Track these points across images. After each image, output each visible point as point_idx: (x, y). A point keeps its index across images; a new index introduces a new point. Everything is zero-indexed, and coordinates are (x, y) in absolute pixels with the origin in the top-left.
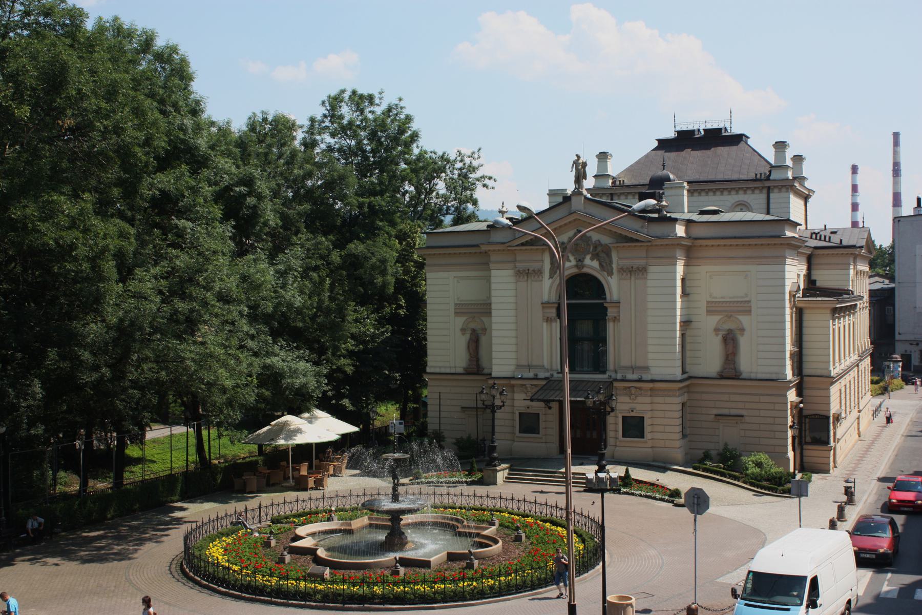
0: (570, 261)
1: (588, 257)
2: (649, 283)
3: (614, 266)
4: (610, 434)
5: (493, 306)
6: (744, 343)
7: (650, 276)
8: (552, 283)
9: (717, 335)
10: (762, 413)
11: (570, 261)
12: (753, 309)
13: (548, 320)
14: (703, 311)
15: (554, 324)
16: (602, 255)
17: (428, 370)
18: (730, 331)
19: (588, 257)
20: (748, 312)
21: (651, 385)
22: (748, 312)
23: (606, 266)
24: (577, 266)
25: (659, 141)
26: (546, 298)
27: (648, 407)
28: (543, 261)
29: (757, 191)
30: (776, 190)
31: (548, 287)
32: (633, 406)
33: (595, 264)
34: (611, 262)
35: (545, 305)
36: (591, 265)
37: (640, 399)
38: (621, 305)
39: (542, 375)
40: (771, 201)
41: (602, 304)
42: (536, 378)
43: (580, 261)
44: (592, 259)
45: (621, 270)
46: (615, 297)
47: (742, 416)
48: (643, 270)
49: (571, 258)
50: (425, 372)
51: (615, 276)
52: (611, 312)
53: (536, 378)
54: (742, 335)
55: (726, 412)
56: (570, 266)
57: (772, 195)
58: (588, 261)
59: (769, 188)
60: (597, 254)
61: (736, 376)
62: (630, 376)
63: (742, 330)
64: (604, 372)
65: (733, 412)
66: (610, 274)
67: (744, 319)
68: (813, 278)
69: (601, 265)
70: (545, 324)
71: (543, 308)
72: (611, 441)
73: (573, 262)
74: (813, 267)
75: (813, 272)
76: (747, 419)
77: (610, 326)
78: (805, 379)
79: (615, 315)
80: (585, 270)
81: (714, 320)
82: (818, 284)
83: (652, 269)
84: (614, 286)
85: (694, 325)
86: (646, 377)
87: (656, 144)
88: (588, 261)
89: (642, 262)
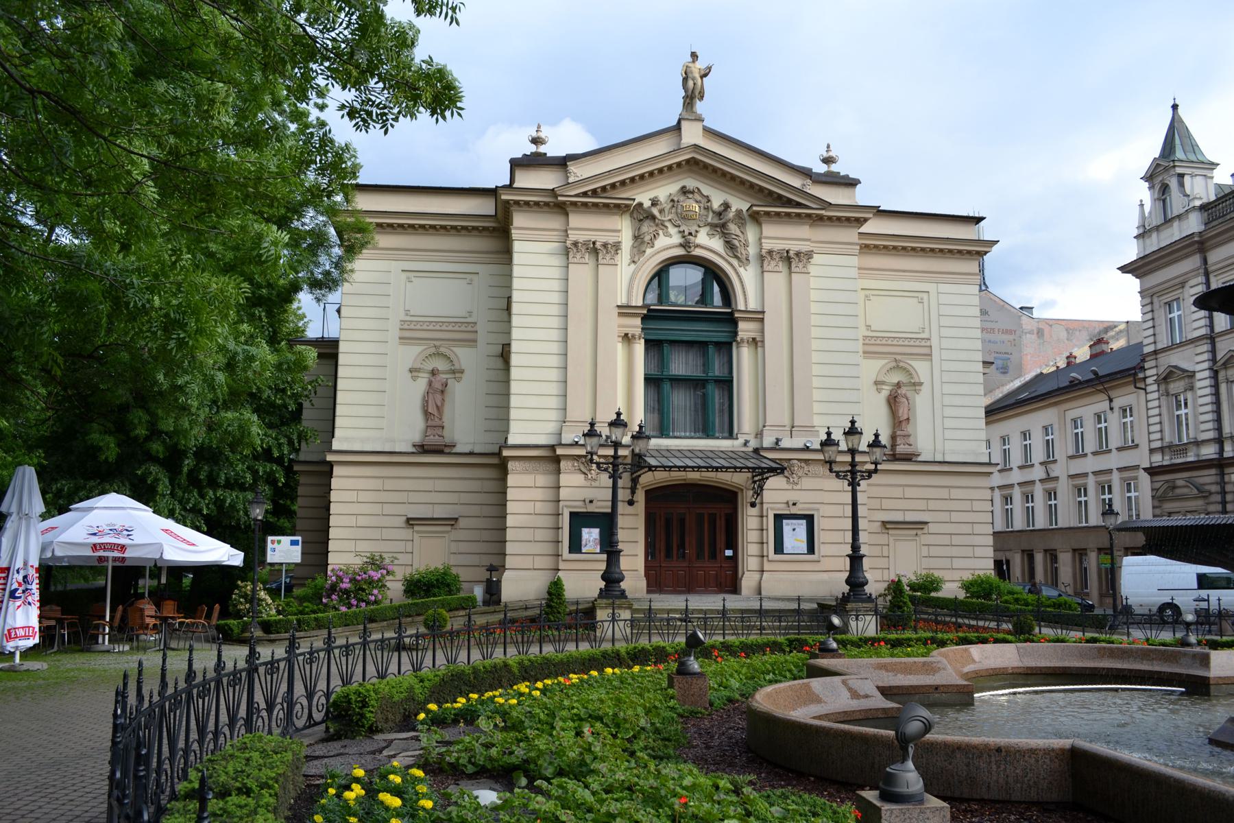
3: (752, 251)
6: (921, 406)
7: (812, 269)
9: (879, 391)
10: (955, 517)
11: (670, 236)
16: (733, 228)
18: (898, 385)
24: (681, 245)
26: (622, 300)
31: (626, 280)
32: (792, 496)
33: (717, 244)
34: (746, 245)
35: (625, 310)
36: (709, 244)
37: (807, 483)
46: (752, 306)
47: (926, 523)
49: (672, 230)
52: (746, 329)
54: (917, 392)
55: (898, 517)
56: (667, 243)
60: (724, 226)
62: (785, 443)
63: (917, 385)
64: (731, 435)
65: (910, 517)
66: (744, 261)
67: (921, 368)
69: (730, 246)
70: (620, 346)
73: (676, 239)
76: (932, 528)
77: (744, 357)
79: (753, 335)
83: (816, 258)
84: (748, 285)
89: (804, 247)
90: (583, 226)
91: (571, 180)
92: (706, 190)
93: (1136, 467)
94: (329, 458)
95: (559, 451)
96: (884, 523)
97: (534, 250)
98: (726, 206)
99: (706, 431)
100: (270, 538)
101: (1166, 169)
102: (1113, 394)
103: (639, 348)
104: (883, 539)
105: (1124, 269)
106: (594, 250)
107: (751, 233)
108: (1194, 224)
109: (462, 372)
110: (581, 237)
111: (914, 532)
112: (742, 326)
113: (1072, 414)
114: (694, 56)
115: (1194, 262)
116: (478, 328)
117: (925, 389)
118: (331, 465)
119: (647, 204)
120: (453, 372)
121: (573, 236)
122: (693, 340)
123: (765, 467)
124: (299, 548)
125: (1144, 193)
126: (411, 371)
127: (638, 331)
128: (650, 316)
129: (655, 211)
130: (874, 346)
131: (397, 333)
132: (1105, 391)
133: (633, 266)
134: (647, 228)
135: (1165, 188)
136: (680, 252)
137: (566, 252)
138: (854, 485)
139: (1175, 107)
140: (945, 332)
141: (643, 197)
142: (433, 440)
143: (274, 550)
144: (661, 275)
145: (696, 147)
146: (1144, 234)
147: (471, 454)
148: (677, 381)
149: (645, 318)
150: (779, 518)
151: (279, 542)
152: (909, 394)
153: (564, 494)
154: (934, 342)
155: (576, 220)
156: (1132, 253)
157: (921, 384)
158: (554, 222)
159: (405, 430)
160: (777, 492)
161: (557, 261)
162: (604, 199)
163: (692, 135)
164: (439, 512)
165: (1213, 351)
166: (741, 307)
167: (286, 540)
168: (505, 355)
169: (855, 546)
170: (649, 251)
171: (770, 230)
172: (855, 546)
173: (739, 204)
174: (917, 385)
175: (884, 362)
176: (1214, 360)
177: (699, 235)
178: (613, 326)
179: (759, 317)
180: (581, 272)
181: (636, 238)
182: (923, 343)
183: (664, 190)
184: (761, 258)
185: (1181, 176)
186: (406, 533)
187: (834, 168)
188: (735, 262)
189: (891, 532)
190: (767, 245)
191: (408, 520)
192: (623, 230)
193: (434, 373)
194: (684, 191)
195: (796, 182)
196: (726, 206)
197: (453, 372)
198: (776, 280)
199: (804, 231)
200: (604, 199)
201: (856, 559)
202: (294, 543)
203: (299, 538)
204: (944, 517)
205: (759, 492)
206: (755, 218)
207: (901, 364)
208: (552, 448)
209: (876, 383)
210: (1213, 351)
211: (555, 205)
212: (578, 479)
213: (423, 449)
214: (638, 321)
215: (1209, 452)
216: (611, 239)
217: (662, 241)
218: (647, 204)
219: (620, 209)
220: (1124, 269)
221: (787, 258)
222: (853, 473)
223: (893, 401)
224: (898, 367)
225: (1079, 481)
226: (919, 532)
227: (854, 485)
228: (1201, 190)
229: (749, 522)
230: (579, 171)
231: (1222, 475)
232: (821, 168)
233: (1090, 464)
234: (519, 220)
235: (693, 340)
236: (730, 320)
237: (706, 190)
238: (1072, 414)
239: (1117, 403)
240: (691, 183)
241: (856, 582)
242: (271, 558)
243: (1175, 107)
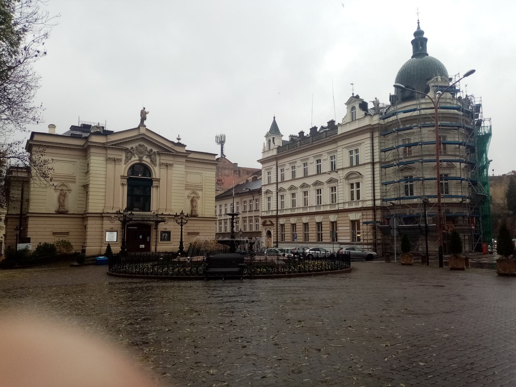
1: (145, 157)
3: (158, 162)
6: (199, 202)
7: (173, 168)
10: (206, 231)
13: (123, 185)
16: (153, 156)
19: (145, 157)
23: (153, 162)
27: (172, 227)
31: (123, 169)
33: (148, 160)
34: (156, 161)
35: (122, 177)
36: (146, 160)
37: (170, 223)
44: (147, 158)
45: (161, 164)
46: (157, 177)
48: (171, 165)
49: (136, 156)
52: (155, 183)
56: (135, 159)
58: (145, 158)
62: (165, 213)
63: (198, 197)
64: (149, 211)
67: (200, 193)
69: (151, 161)
73: (137, 158)
80: (143, 162)
81: (188, 192)
83: (175, 165)
84: (157, 172)
88: (145, 158)
89: (171, 162)
90: (112, 154)
91: (109, 141)
92: (146, 145)
93: (258, 216)
95: (103, 215)
96: (188, 233)
97: (97, 161)
98: (151, 150)
99: (144, 210)
101: (270, 136)
102: (254, 195)
103: (126, 188)
104: (188, 237)
105: (258, 161)
106: (115, 160)
107: (158, 158)
108: (275, 152)
109: (71, 190)
112: (154, 182)
113: (244, 199)
114: (144, 108)
115: (275, 163)
116: (76, 178)
117: (200, 199)
119: (130, 148)
120: (68, 190)
121: (109, 156)
122: (140, 186)
123: (159, 219)
125: (265, 140)
127: (126, 183)
128: (129, 180)
129: (132, 151)
130: (187, 187)
132: (252, 194)
134: (129, 154)
135: (270, 141)
136: (138, 162)
137: (107, 160)
138: (182, 226)
139: (274, 118)
140: (206, 184)
141: (129, 147)
142: (62, 210)
144: (133, 167)
145: (144, 134)
146: (264, 152)
147: (73, 214)
149: (128, 179)
153: (104, 226)
155: (109, 152)
156: (260, 157)
158: (104, 152)
159: (52, 206)
160: (162, 227)
161: (105, 162)
162: (118, 146)
163: (142, 131)
164: (63, 231)
165: (277, 187)
168: (86, 187)
169: (181, 240)
170: (130, 161)
171: (163, 157)
172: (181, 240)
173: (155, 150)
174: (198, 197)
176: (277, 189)
178: (119, 181)
179: (158, 180)
180: (111, 166)
181: (126, 157)
183: (134, 145)
184: (160, 165)
185: (273, 138)
186: (53, 237)
187: (180, 141)
190: (162, 161)
191: (54, 233)
192: (123, 156)
193: (62, 190)
194: (140, 145)
195: (170, 145)
196: (151, 150)
197: (68, 190)
198: (164, 171)
199: (171, 158)
201: (181, 243)
204: (204, 231)
205: (157, 225)
206: (159, 154)
208: (101, 214)
210: (277, 187)
211: (104, 147)
212: (109, 222)
213: (58, 212)
214: (126, 180)
215: (274, 213)
216: (119, 158)
217: (133, 159)
218: (130, 148)
219: (122, 150)
220: (258, 161)
221: (167, 165)
222: (182, 223)
223: (192, 201)
224: (194, 193)
225: (245, 219)
227: (182, 226)
228: (278, 143)
229: (153, 233)
230: (112, 138)
231: (277, 219)
232: (176, 141)
233: (247, 215)
234: (92, 150)
235: (140, 186)
236: (151, 181)
237: (146, 145)
238: (244, 199)
239: (255, 198)
240: (142, 143)
241: (181, 247)
243: (274, 118)
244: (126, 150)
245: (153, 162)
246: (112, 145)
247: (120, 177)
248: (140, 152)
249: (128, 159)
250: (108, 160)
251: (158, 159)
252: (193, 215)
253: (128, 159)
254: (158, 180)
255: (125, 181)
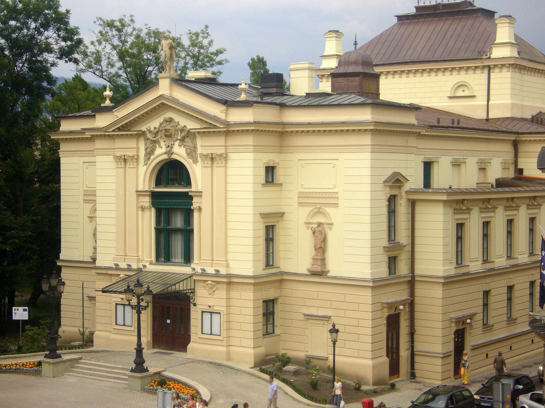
0: (161, 147)
1: (177, 143)
2: (230, 171)
4: (193, 329)
5: (98, 193)
7: (230, 164)
8: (147, 169)
11: (161, 147)
12: (340, 202)
13: (143, 209)
14: (295, 201)
15: (147, 213)
17: (62, 256)
18: (319, 224)
19: (177, 143)
20: (336, 205)
21: (225, 280)
22: (336, 205)
23: (192, 153)
24: (165, 153)
25: (400, 18)
26: (141, 188)
28: (138, 148)
29: (478, 71)
30: (497, 70)
31: (142, 177)
35: (140, 193)
36: (180, 153)
38: (203, 194)
39: (134, 266)
40: (492, 81)
41: (187, 193)
42: (129, 268)
43: (170, 147)
46: (200, 189)
48: (225, 157)
50: (58, 258)
51: (200, 164)
53: (129, 268)
54: (331, 229)
56: (160, 153)
57: (492, 74)
59: (489, 68)
61: (322, 274)
62: (210, 270)
66: (195, 161)
68: (520, 166)
71: (138, 195)
72: (193, 337)
73: (164, 150)
74: (520, 154)
75: (520, 160)
78: (416, 279)
80: (174, 157)
82: (526, 173)
83: (232, 156)
85: (286, 217)
86: (223, 271)
87: (395, 20)
94: (58, 264)
100: (14, 308)
110: (118, 154)
111: (322, 322)
112: (195, 200)
118: (60, 268)
124: (27, 312)
126: (89, 217)
128: (154, 196)
131: (82, 197)
133: (145, 167)
136: (165, 157)
143: (16, 313)
145: (161, 96)
148: (177, 230)
150: (202, 312)
151: (18, 310)
152: (327, 230)
154: (340, 195)
157: (332, 224)
161: (113, 165)
166: (193, 189)
167: (21, 309)
170: (152, 157)
175: (310, 209)
177: (174, 146)
181: (146, 149)
182: (334, 196)
183: (154, 124)
188: (191, 161)
189: (310, 321)
199: (220, 141)
200: (126, 129)
202: (25, 310)
203: (27, 308)
206: (203, 134)
207: (321, 210)
209: (306, 223)
224: (319, 212)
226: (326, 323)
236: (188, 197)
242: (15, 317)
244: (143, 134)
245: (192, 153)
246: (114, 131)
247: (135, 194)
248: (168, 133)
249: (149, 153)
250: (118, 159)
251: (203, 146)
252: (319, 273)
253: (149, 153)
254: (199, 194)
255: (146, 201)
